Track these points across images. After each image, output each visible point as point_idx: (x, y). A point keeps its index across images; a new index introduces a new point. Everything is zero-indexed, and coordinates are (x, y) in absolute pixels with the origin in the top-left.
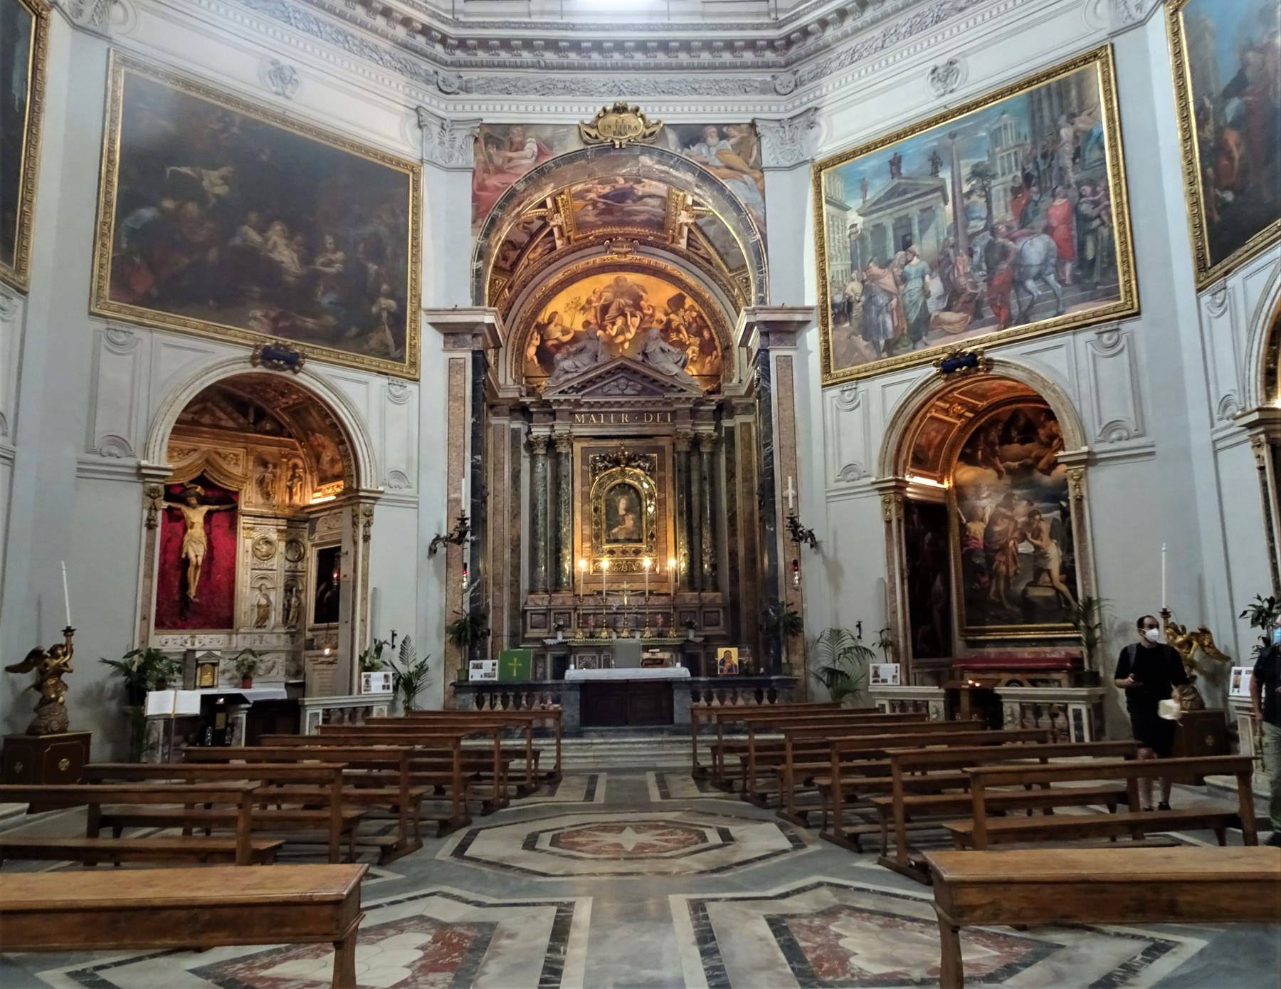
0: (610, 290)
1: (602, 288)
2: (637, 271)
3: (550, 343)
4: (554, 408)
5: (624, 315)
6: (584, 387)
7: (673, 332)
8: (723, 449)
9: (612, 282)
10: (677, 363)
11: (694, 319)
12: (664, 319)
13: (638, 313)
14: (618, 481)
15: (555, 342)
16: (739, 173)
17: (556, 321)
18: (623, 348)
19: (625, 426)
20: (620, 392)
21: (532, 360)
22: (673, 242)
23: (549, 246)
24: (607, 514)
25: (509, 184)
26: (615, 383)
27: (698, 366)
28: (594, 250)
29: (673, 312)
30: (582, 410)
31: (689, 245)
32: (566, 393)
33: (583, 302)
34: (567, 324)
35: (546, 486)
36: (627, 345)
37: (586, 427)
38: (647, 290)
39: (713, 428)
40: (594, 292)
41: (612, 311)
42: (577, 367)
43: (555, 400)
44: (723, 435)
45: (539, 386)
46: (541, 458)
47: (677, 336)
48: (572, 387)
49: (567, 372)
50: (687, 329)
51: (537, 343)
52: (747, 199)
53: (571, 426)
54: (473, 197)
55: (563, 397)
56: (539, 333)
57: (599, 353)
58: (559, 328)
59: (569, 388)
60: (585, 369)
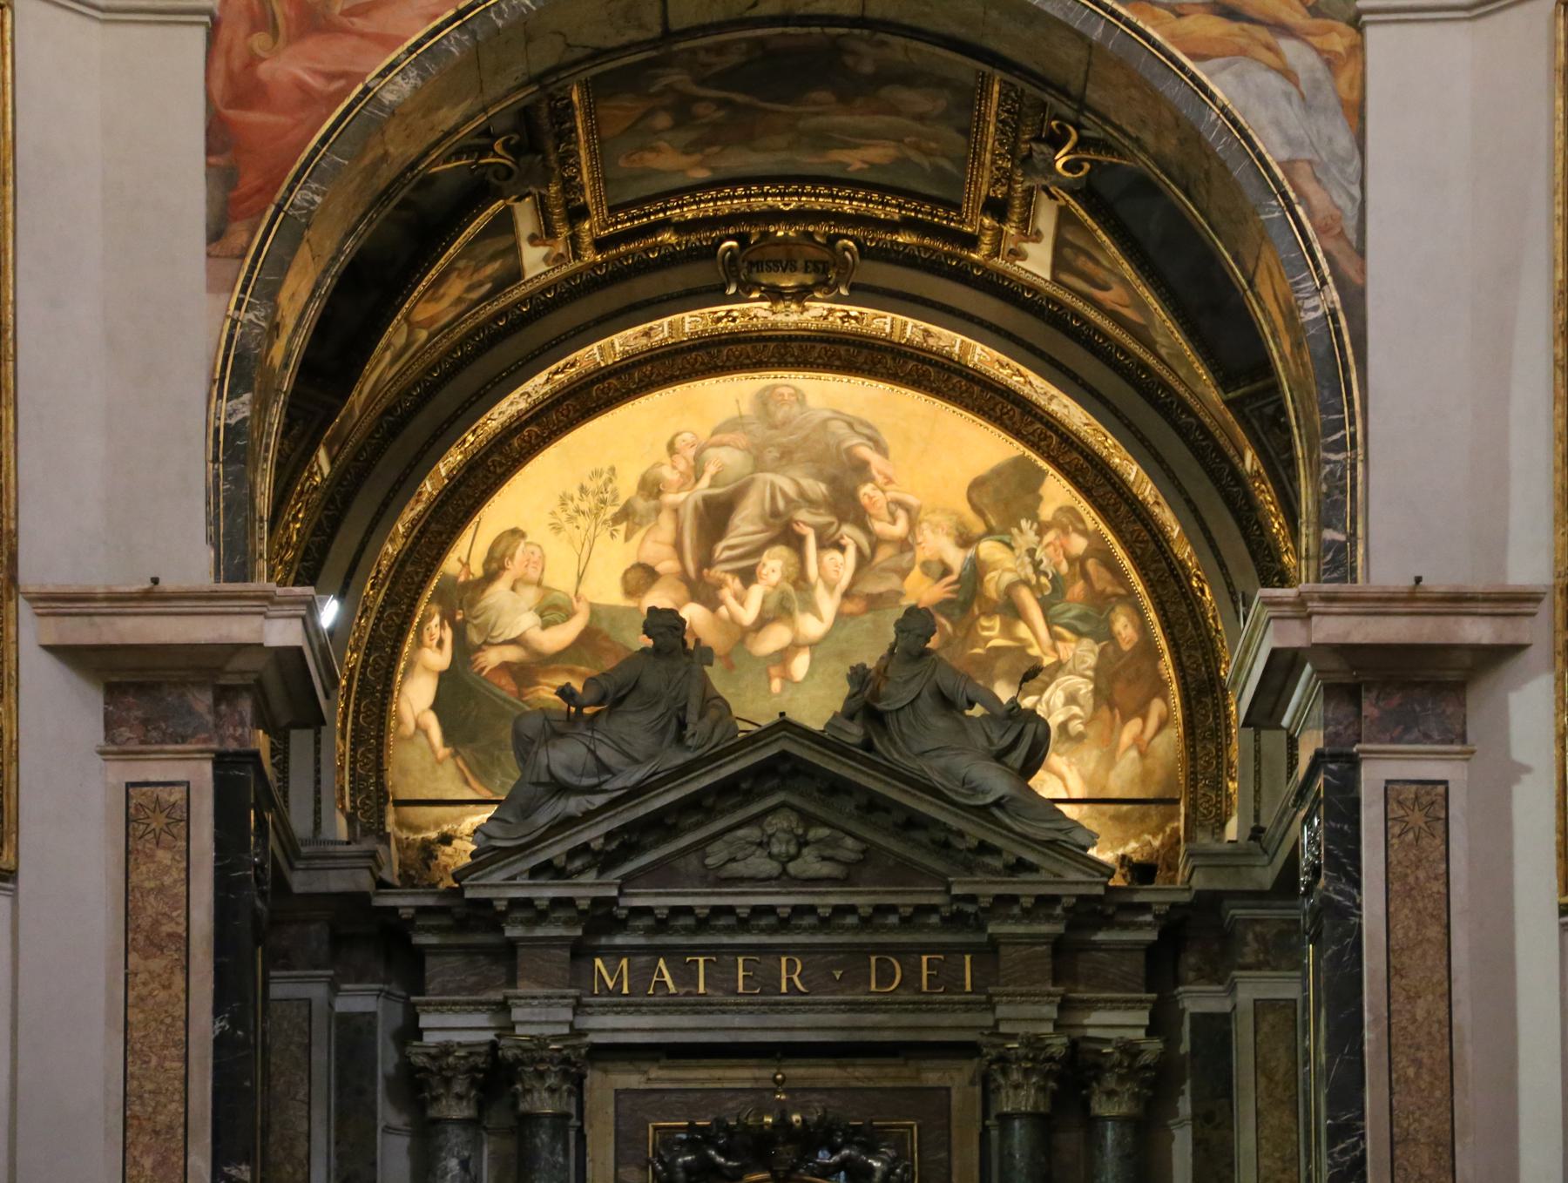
0: (743, 440)
1: (704, 434)
2: (848, 367)
3: (492, 658)
4: (512, 932)
5: (794, 541)
7: (989, 614)
9: (746, 408)
10: (1000, 756)
11: (1077, 562)
12: (956, 558)
13: (850, 534)
15: (512, 654)
16: (1262, 34)
17: (514, 569)
18: (786, 678)
19: (793, 1007)
20: (771, 867)
21: (421, 729)
22: (996, 253)
23: (492, 268)
25: (352, 78)
27: (1090, 756)
28: (676, 279)
29: (990, 532)
30: (619, 940)
31: (1059, 263)
33: (627, 487)
34: (561, 580)
36: (800, 665)
37: (637, 1008)
38: (887, 438)
40: (672, 448)
41: (745, 526)
42: (603, 768)
43: (514, 903)
45: (446, 839)
47: (1007, 631)
48: (585, 848)
50: (1045, 606)
51: (438, 659)
52: (1290, 141)
53: (579, 1007)
54: (209, 132)
55: (546, 892)
56: (448, 617)
57: (692, 717)
58: (530, 595)
59: (572, 854)
60: (636, 775)
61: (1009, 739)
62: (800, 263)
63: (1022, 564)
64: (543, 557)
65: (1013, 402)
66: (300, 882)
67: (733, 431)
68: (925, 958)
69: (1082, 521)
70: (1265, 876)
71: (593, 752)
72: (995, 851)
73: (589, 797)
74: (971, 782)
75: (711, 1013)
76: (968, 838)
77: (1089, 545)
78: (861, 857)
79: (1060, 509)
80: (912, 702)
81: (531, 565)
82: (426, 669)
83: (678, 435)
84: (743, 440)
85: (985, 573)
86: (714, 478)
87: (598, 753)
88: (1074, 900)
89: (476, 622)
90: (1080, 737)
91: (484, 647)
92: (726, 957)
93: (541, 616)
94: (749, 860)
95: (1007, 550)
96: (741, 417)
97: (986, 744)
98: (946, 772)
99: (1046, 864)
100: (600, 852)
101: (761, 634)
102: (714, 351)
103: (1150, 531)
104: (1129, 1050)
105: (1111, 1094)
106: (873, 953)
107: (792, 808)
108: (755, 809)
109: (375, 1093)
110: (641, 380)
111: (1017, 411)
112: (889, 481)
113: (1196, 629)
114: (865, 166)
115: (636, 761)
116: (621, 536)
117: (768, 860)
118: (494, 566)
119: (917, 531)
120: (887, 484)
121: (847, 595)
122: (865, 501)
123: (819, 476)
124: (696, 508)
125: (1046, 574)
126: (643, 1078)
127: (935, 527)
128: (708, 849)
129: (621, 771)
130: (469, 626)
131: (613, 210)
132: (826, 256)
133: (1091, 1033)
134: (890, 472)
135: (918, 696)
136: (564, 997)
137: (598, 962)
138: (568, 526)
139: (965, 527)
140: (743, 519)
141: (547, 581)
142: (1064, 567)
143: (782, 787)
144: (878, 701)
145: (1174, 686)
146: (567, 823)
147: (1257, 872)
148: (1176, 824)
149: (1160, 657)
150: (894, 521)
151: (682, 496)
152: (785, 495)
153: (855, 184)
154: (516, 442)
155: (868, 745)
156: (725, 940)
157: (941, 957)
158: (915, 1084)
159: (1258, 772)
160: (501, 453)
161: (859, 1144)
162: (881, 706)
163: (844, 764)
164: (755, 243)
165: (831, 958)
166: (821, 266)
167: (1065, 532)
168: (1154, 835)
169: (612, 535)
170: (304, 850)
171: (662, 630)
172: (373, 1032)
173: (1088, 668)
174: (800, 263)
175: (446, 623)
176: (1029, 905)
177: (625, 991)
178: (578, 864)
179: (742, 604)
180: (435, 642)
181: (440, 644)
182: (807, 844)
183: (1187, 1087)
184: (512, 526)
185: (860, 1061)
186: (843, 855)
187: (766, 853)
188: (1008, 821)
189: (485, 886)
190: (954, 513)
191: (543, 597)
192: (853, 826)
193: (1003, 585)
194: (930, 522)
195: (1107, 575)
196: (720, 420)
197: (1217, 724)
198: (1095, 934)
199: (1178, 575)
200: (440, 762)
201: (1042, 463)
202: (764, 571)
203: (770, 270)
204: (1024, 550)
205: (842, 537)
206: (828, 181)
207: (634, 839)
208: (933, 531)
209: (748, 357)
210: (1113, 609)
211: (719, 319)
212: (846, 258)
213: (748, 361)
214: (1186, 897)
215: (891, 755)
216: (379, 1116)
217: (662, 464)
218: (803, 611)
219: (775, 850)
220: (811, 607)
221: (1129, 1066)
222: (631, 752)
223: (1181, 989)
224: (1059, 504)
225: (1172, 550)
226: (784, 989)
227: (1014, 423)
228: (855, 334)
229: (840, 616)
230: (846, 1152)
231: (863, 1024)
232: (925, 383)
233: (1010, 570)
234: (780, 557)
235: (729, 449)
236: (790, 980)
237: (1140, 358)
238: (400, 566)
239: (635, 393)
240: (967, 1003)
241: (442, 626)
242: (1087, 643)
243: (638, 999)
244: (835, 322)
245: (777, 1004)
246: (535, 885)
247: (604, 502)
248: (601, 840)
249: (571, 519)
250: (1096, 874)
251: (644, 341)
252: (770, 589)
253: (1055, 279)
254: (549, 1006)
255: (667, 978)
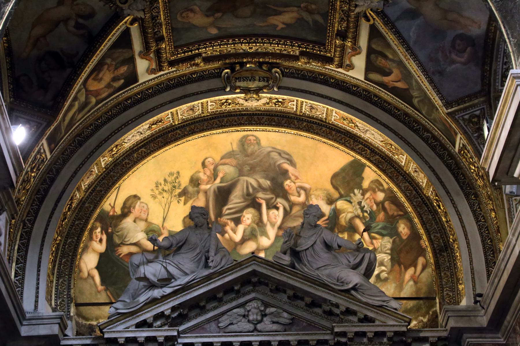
0: (234, 162)
1: (218, 158)
3: (125, 250)
5: (257, 207)
6: (183, 318)
7: (342, 232)
9: (235, 147)
10: (355, 267)
11: (381, 205)
13: (281, 202)
15: (133, 249)
17: (136, 212)
20: (250, 327)
21: (90, 276)
23: (123, 69)
26: (241, 311)
29: (341, 197)
32: (150, 325)
33: (185, 181)
34: (156, 219)
38: (295, 159)
40: (204, 165)
48: (161, 315)
49: (152, 286)
51: (102, 248)
56: (104, 229)
57: (212, 253)
58: (142, 225)
59: (157, 317)
60: (187, 279)
61: (358, 260)
62: (257, 78)
63: (356, 209)
64: (148, 209)
65: (349, 137)
66: (25, 331)
67: (230, 158)
69: (382, 185)
70: (483, 320)
71: (166, 268)
72: (354, 313)
73: (165, 289)
74: (342, 279)
76: (341, 307)
77: (385, 196)
78: (291, 322)
79: (372, 182)
80: (312, 246)
81: (143, 212)
82: (94, 251)
83: (206, 159)
84: (234, 162)
85: (340, 215)
86: (222, 179)
87: (168, 268)
88: (393, 334)
89: (117, 234)
90: (386, 279)
91: (121, 245)
93: (147, 234)
94: (239, 324)
95: (349, 204)
96: (233, 151)
97: (348, 262)
98: (329, 276)
99: (379, 317)
100: (168, 317)
101: (244, 245)
102: (221, 119)
103: (412, 186)
107: (258, 299)
108: (242, 300)
110: (189, 131)
111: (352, 141)
112: (297, 178)
113: (436, 225)
114: (284, 26)
115: (186, 274)
116: (182, 203)
117: (248, 324)
118: (126, 210)
119: (309, 199)
120: (296, 180)
121: (280, 228)
122: (287, 187)
123: (266, 178)
124: (215, 191)
125: (366, 212)
127: (317, 197)
128: (220, 320)
129: (179, 278)
130: (114, 235)
131: (176, 47)
132: (268, 75)
134: (297, 174)
135: (315, 243)
138: (159, 197)
139: (330, 196)
140: (235, 197)
141: (149, 220)
142: (375, 207)
143: (253, 291)
144: (297, 247)
145: (429, 249)
146: (154, 301)
147: (479, 319)
148: (435, 309)
149: (420, 238)
150: (299, 196)
151: (208, 186)
152: (253, 187)
153: (280, 37)
154: (135, 155)
155: (293, 266)
159: (473, 278)
160: (129, 159)
162: (298, 249)
163: (282, 275)
164: (238, 70)
166: (266, 79)
167: (374, 192)
168: (424, 316)
169: (178, 202)
170: (28, 316)
171: (198, 215)
173: (388, 250)
174: (257, 78)
175: (104, 232)
176: (371, 336)
178: (159, 323)
179: (235, 233)
180: (98, 239)
181: (101, 241)
182: (265, 315)
184: (134, 193)
186: (282, 320)
187: (247, 320)
188: (359, 297)
189: (114, 332)
190: (325, 190)
191: (148, 226)
192: (286, 307)
193: (348, 219)
194: (315, 195)
195: (394, 207)
196: (224, 152)
197: (450, 264)
199: (426, 203)
200: (99, 292)
201: (364, 161)
202: (244, 219)
203: (244, 81)
204: (356, 203)
205: (277, 204)
206: (268, 36)
207: (185, 312)
208: (316, 199)
209: (235, 122)
210: (398, 222)
211: (223, 104)
212: (276, 76)
213: (236, 123)
214: (445, 334)
215: (304, 270)
217: (200, 172)
218: (261, 235)
219: (251, 318)
220: (265, 233)
222: (183, 269)
224: (371, 179)
225: (423, 193)
227: (350, 145)
228: (281, 112)
229: (277, 237)
232: (312, 130)
233: (351, 212)
234: (251, 213)
235: (228, 166)
237: (404, 111)
238: (83, 204)
239: (187, 136)
241: (102, 233)
242: (387, 239)
244: (272, 107)
246: (137, 331)
247: (174, 187)
248: (170, 311)
249: (160, 193)
250: (402, 321)
251: (191, 112)
252: (247, 226)
253: (366, 78)
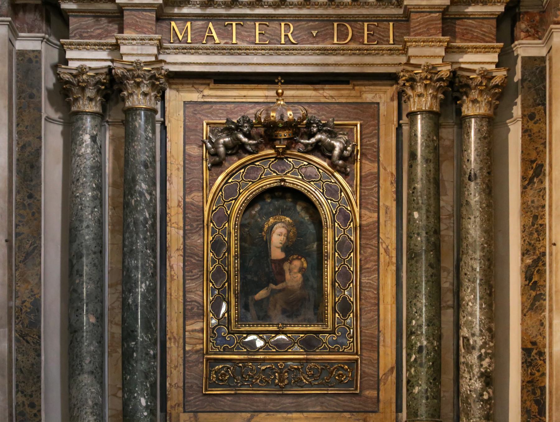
8: (517, 111)
14: (270, 182)
19: (288, 51)
24: (243, 254)
30: (185, 10)
35: (100, 188)
37: (195, 51)
39: (494, 57)
44: (518, 77)
46: (88, 122)
68: (366, 24)
75: (240, 54)
92: (248, 23)
104: (487, 76)
105: (474, 101)
106: (336, 21)
109: (40, 97)
126: (200, 96)
133: (463, 66)
136: (151, 39)
137: (173, 24)
156: (248, 11)
157: (376, 24)
158: (359, 101)
161: (326, 131)
165: (311, 23)
172: (39, 62)
177: (189, 41)
183: (519, 100)
185: (327, 86)
198: (467, 8)
216: (43, 111)
221: (486, 86)
223: (516, 43)
226: (283, 42)
230: (318, 136)
231: (329, 62)
236: (286, 36)
240: (390, 50)
243: (197, 45)
245: (278, 49)
254: (143, 45)
255: (214, 34)
